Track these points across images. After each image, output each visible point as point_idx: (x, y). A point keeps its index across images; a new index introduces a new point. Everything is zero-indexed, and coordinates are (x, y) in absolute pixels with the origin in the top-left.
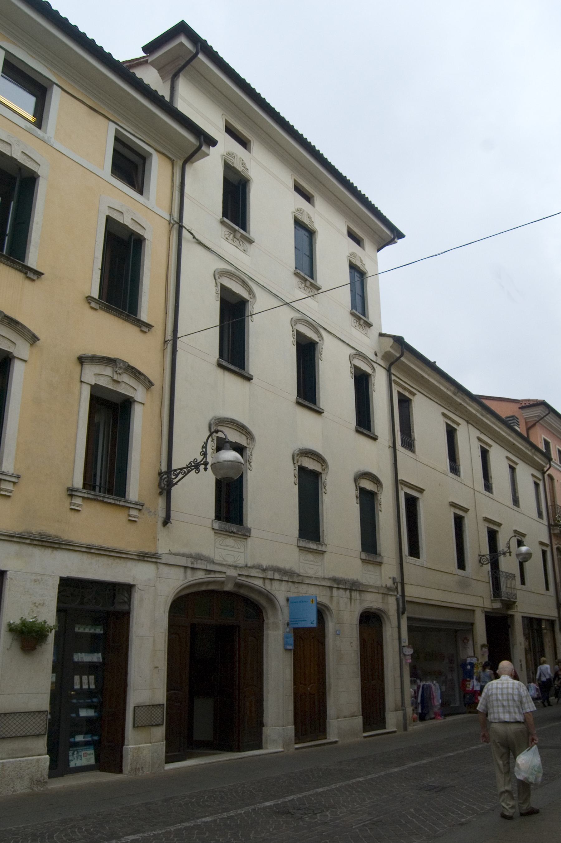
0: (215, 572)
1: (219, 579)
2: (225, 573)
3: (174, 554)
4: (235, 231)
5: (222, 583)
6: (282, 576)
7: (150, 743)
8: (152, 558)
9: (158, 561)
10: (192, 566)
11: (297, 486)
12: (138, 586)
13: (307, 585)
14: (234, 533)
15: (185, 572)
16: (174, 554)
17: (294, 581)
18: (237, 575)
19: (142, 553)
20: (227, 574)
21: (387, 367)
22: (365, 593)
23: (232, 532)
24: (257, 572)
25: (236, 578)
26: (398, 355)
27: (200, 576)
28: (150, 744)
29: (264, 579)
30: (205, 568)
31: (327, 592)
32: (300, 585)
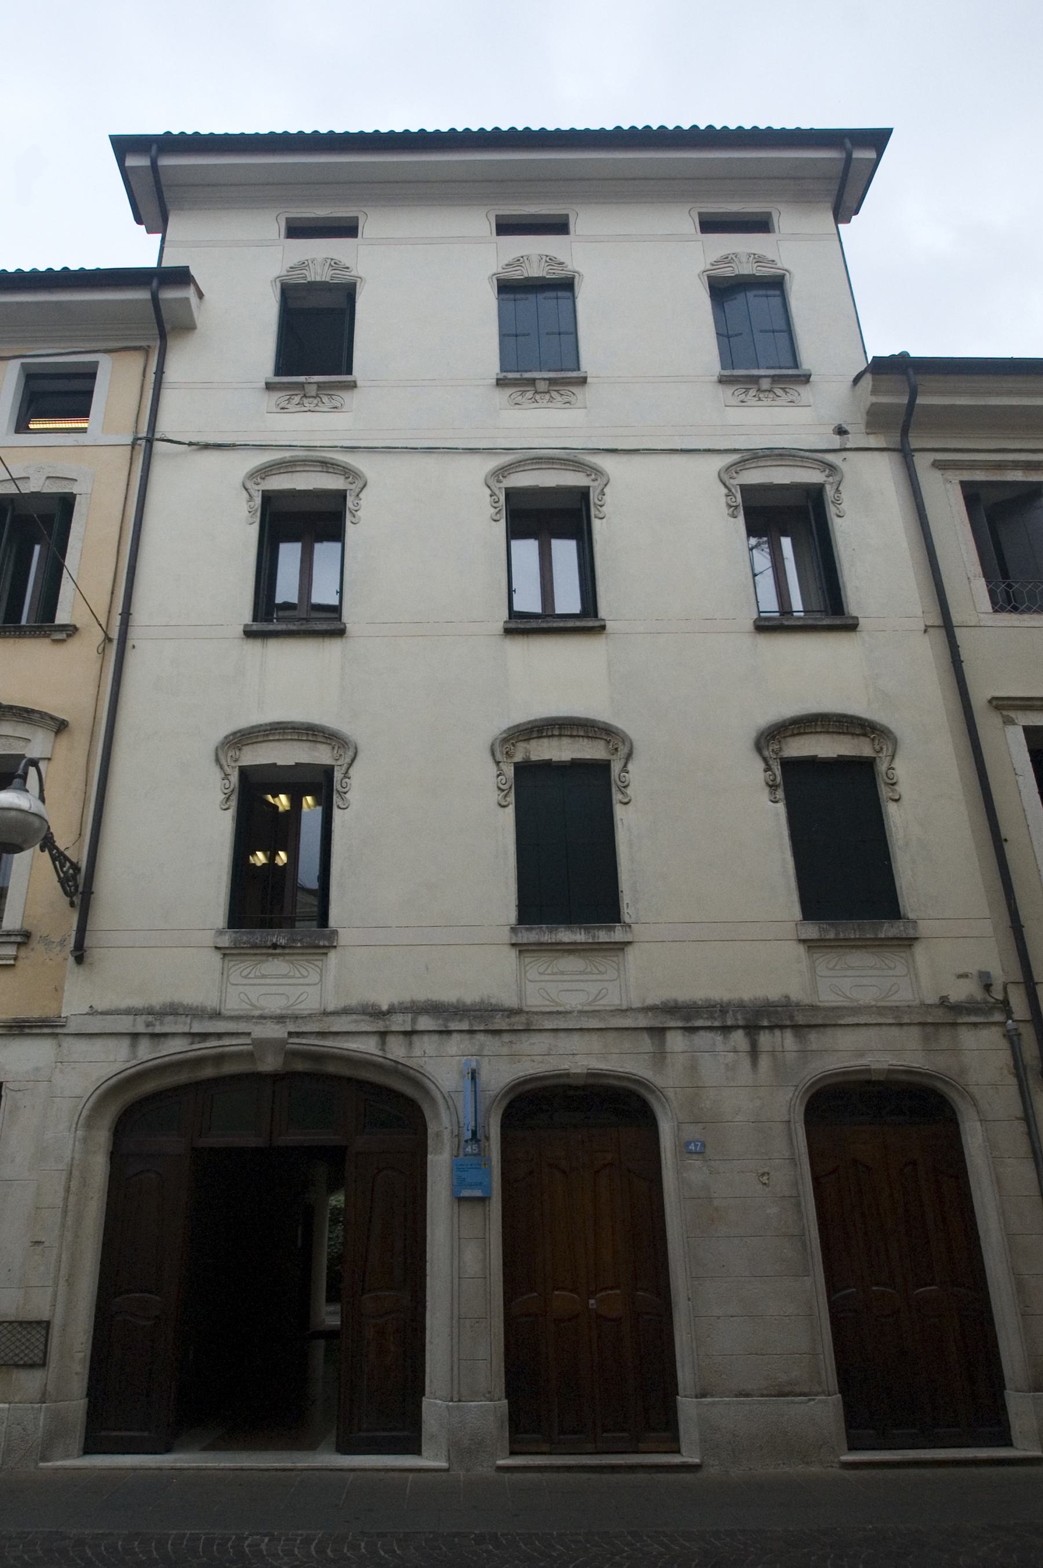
0: (219, 1035)
1: (227, 1049)
2: (249, 1034)
3: (102, 1013)
4: (301, 386)
5: (250, 1055)
6: (447, 1020)
7: (10, 1403)
8: (40, 1027)
9: (58, 1031)
10: (150, 1030)
11: (511, 810)
12: (8, 1085)
13: (552, 1034)
14: (283, 947)
15: (134, 1046)
16: (102, 1013)
17: (497, 1027)
18: (286, 1035)
19: (15, 1020)
20: (253, 1036)
21: (895, 440)
22: (829, 1031)
23: (275, 946)
24: (356, 1021)
25: (283, 1042)
26: (905, 400)
27: (175, 1048)
28: (7, 1406)
29: (383, 1035)
30: (186, 1029)
31: (646, 1043)
32: (524, 1037)
